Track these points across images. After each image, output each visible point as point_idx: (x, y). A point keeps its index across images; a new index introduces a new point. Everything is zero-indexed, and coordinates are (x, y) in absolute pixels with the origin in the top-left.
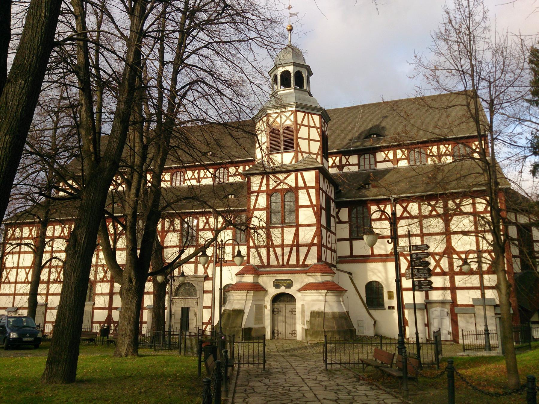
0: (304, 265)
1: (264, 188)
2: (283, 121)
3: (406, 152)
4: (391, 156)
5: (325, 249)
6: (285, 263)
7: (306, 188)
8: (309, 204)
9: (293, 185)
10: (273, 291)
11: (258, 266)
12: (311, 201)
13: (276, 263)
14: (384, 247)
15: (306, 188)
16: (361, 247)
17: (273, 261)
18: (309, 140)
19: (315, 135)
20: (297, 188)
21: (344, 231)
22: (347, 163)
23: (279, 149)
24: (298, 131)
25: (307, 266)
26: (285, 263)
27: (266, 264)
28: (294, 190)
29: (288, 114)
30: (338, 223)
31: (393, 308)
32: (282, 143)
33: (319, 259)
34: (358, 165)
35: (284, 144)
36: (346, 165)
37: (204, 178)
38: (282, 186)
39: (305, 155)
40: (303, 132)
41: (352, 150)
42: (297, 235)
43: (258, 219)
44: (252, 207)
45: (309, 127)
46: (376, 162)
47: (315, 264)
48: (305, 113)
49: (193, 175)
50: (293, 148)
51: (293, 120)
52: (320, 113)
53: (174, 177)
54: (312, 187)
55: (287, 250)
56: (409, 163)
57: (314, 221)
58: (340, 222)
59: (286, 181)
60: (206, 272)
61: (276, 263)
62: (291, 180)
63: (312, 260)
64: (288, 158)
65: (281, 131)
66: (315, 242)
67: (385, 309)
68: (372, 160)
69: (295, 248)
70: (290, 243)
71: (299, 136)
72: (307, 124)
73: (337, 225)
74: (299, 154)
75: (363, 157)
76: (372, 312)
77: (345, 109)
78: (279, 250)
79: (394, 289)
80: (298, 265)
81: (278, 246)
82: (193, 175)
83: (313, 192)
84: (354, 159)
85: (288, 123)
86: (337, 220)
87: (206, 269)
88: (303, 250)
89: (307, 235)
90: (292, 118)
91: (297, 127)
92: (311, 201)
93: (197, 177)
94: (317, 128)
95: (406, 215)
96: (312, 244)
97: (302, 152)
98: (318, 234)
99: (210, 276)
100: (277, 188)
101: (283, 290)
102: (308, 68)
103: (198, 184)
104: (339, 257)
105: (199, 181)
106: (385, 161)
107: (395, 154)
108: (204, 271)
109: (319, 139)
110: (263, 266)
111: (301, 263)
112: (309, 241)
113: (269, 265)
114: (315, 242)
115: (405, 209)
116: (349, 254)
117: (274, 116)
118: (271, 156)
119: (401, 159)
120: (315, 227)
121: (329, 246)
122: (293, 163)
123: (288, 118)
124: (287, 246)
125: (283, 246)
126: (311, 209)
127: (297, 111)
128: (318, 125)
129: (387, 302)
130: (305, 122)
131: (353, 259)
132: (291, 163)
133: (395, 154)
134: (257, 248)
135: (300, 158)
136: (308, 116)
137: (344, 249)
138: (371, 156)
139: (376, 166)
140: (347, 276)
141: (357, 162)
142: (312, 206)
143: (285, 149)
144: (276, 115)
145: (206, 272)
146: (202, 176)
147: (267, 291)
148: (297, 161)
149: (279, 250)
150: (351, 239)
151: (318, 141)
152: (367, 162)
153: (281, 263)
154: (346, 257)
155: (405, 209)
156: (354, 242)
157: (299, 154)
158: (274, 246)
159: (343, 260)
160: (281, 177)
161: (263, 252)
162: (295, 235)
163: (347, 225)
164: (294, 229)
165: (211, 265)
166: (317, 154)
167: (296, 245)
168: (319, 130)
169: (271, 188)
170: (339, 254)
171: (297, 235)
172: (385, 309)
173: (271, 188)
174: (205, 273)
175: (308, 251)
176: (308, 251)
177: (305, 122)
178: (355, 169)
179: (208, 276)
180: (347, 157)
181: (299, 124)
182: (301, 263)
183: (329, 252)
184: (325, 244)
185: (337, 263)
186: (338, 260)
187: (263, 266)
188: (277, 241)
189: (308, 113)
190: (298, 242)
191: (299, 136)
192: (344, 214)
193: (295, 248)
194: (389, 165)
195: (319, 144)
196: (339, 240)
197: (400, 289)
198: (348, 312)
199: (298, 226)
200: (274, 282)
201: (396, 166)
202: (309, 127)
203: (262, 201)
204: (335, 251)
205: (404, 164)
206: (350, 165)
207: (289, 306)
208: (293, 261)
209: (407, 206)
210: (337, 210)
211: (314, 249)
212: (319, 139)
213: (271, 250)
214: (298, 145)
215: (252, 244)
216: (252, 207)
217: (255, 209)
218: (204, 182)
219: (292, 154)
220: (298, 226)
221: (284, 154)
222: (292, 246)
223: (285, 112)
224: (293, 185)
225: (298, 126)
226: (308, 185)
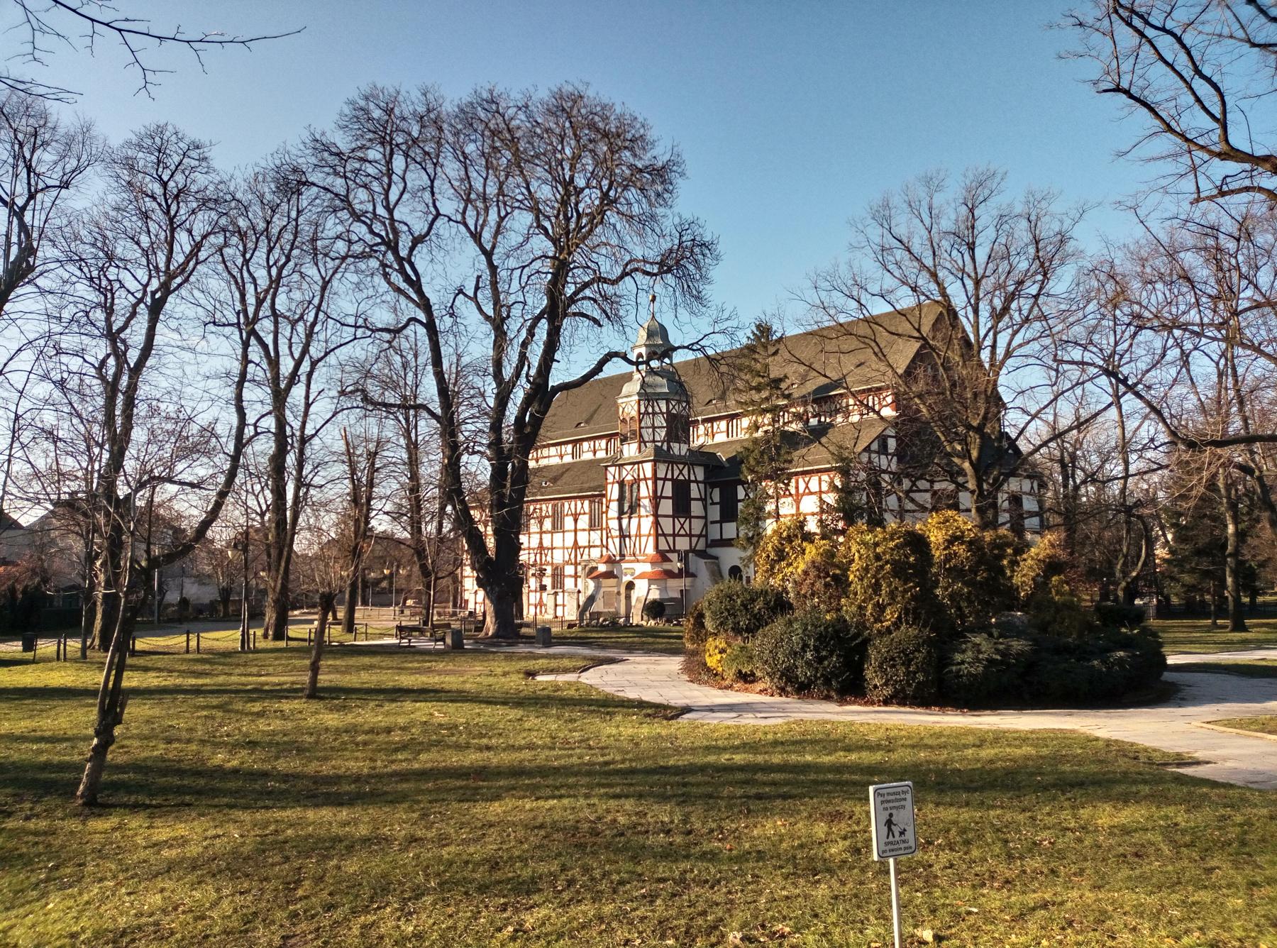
7: (645, 479)
16: (730, 530)
18: (654, 428)
19: (660, 421)
21: (715, 513)
24: (640, 421)
58: (713, 503)
88: (644, 540)
97: (645, 443)
128: (664, 410)
137: (714, 533)
150: (721, 522)
166: (663, 442)
196: (713, 522)
199: (640, 517)
203: (614, 492)
220: (640, 517)
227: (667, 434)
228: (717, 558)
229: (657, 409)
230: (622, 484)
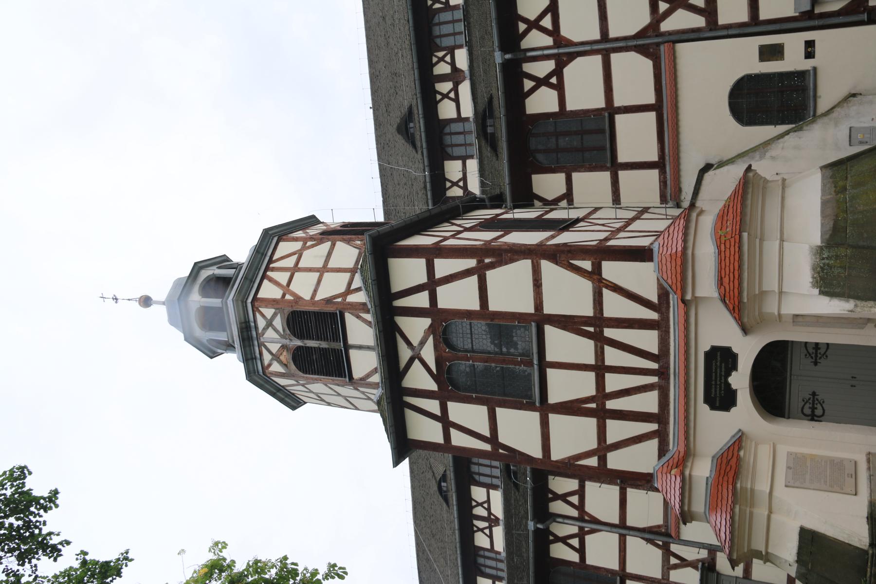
0: (661, 306)
1: (433, 406)
2: (276, 336)
3: (441, 54)
4: (445, 87)
5: (622, 235)
6: (654, 366)
7: (432, 285)
8: (474, 279)
9: (426, 322)
10: (745, 413)
11: (662, 451)
12: (467, 273)
13: (654, 395)
14: (634, 77)
15: (432, 285)
16: (636, 137)
17: (648, 402)
18: (324, 270)
20: (433, 311)
21: (591, 185)
22: (461, 184)
23: (337, 353)
24: (298, 299)
25: (663, 295)
26: (654, 366)
27: (654, 427)
28: (443, 322)
29: (261, 323)
30: (571, 202)
31: (810, 45)
32: (324, 345)
33: (641, 254)
34: (464, 159)
35: (325, 339)
36: (465, 188)
37: (489, 509)
38: (428, 353)
39: (357, 282)
40: (303, 286)
41: (431, 171)
42: (568, 323)
43: (519, 429)
44: (487, 447)
45: (296, 269)
46: (460, 119)
47: (660, 270)
48: (264, 276)
49: (482, 530)
50: (333, 315)
51: (272, 311)
52: (276, 239)
53: (488, 571)
55: (613, 357)
56: (460, 47)
57: (525, 266)
58: (568, 196)
59: (415, 342)
60: (693, 565)
61: (654, 395)
62: (415, 328)
63: (641, 278)
64: (360, 332)
65: (298, 343)
66: (587, 265)
67: (815, 69)
68: (456, 127)
69: (610, 333)
70: (590, 344)
71: (307, 296)
72: (287, 275)
73: (576, 205)
74: (351, 298)
75: (449, 150)
76: (823, 105)
77: (383, 197)
78: (613, 382)
79: (754, 43)
80: (660, 326)
81: (600, 383)
82: (482, 530)
83: (444, 267)
84: (453, 169)
85: (278, 323)
86: (564, 203)
87: (684, 563)
88: (615, 306)
89: (567, 292)
90: (269, 312)
91: (289, 301)
92: (467, 273)
93: (486, 524)
94: (304, 248)
95: (547, 22)
96: (595, 276)
97: (349, 291)
98: (563, 256)
99: (704, 554)
100: (433, 368)
101: (740, 380)
102: (198, 267)
103: (501, 523)
104: (663, 199)
105: (496, 521)
106: (457, 100)
107: (443, 78)
108: (689, 570)
109: (329, 243)
110: (661, 435)
111: (653, 315)
112: (586, 286)
113: (660, 418)
114: (587, 265)
115: (535, 25)
116: (655, 173)
117: (267, 357)
119: (453, 64)
120: (546, 266)
121: (618, 225)
122: (369, 317)
123: (269, 324)
124: (600, 354)
125: (600, 369)
126: (490, 274)
127: (255, 298)
128: (298, 245)
129: (793, 60)
130: (282, 277)
131: (666, 163)
132: (369, 323)
133: (443, 78)
134: (603, 449)
135: (360, 297)
136: (273, 269)
137: (641, 187)
138: (447, 130)
139: (467, 119)
140: (709, 176)
141: (459, 163)
142: (480, 271)
143: (336, 339)
144: (264, 351)
145: (693, 565)
146: (484, 513)
147: (740, 430)
149: (613, 382)
150: (615, 167)
151: (333, 245)
152: (459, 139)
153: (654, 379)
154: (663, 183)
155: (535, 25)
156: (622, 158)
157: (351, 298)
158: (602, 395)
159: (669, 193)
160: (405, 353)
161: (616, 430)
162: (564, 328)
163: (575, 176)
164: (549, 329)
165: (674, 548)
167: (593, 326)
168: (309, 243)
169: (433, 386)
170: (654, 198)
171: (568, 323)
172: (815, 69)
173: (433, 386)
174: (696, 568)
175: (616, 289)
176: (616, 289)
177: (282, 277)
178: (473, 165)
179: (703, 561)
180: (448, 184)
181: (284, 296)
182: (653, 315)
183: (637, 225)
184: (603, 236)
185: (678, 206)
186: (670, 204)
187: (661, 435)
188: (583, 386)
189: (267, 269)
190: (586, 321)
191: (307, 296)
192: (548, 184)
193: (609, 333)
194: (465, 89)
195: (340, 246)
197: (755, 25)
198: (823, 168)
200: (713, 407)
201: (467, 73)
202: (296, 269)
203: (469, 415)
204: (646, 210)
205: (462, 58)
206: (464, 178)
207: (799, 365)
208: (648, 340)
209: (525, 20)
210: (537, 203)
211: (612, 270)
212: (329, 243)
213: (611, 405)
214: (329, 301)
215: (593, 462)
216: (487, 447)
217: (493, 439)
218: (498, 509)
219: (349, 318)
220: (540, 319)
221: (351, 341)
222: (601, 341)
223: (256, 328)
224: (426, 322)
225: (288, 297)
226: (423, 279)
227: (348, 242)
228: (708, 167)
229: (290, 262)
230: (450, 386)
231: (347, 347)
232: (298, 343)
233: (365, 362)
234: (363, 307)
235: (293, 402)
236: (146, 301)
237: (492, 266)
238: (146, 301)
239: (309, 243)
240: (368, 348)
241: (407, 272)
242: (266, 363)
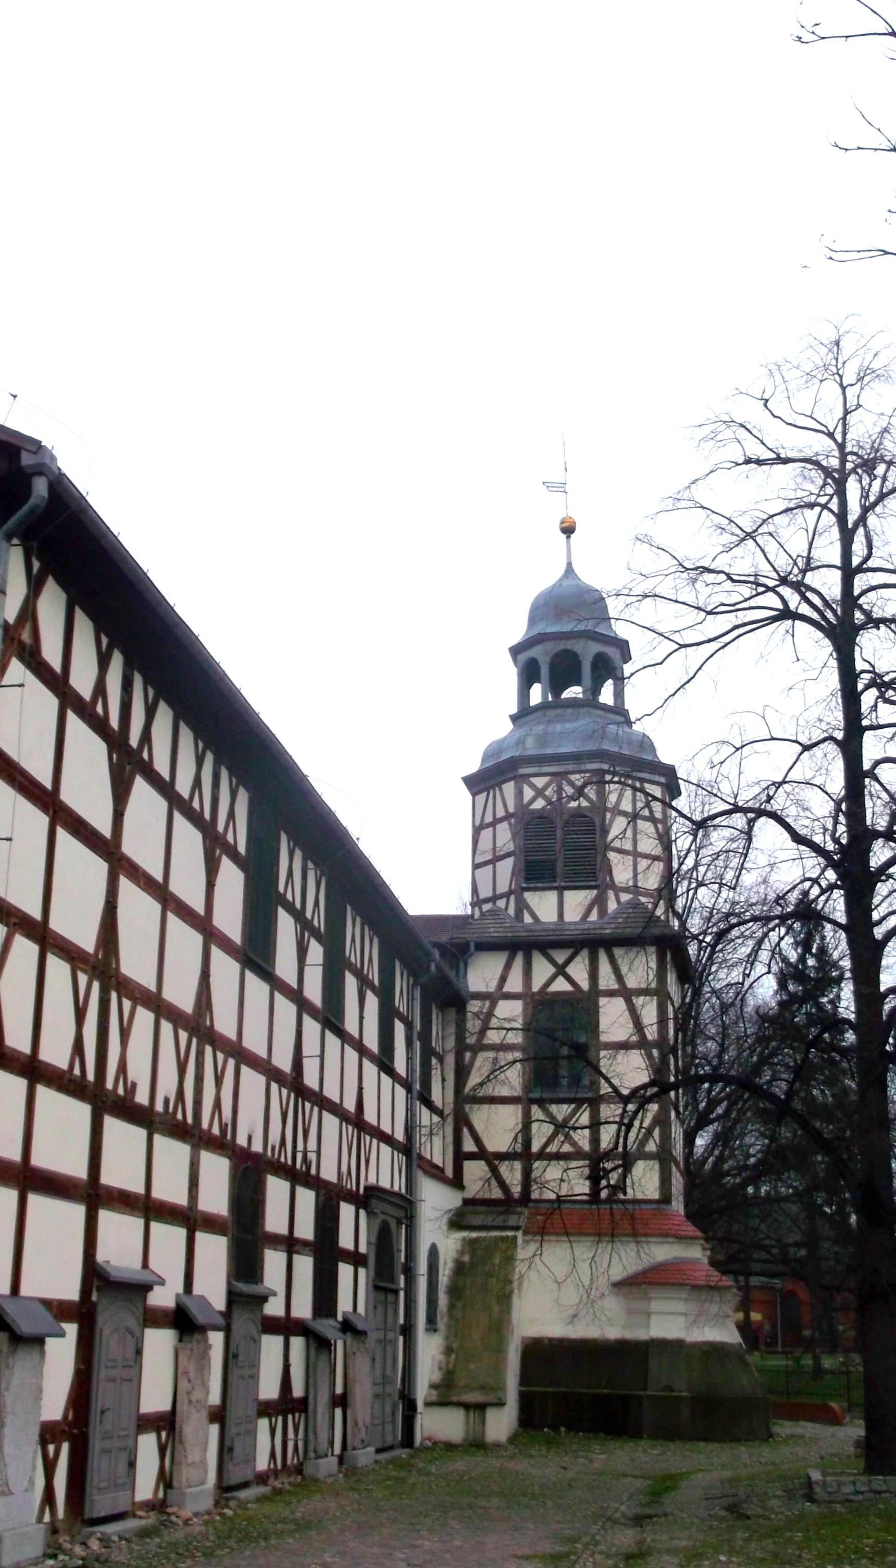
18: (636, 854)
39: (625, 897)
50: (593, 875)
54: (645, 992)
65: (559, 826)
74: (611, 894)
97: (618, 890)
117: (540, 782)
118: (527, 895)
122: (594, 916)
130: (626, 806)
135: (612, 906)
142: (643, 1044)
144: (546, 779)
148: (603, 912)
177: (626, 806)
217: (480, 1047)
225: (608, 815)
231: (561, 890)
232: (559, 826)
233: (544, 906)
234: (603, 912)
235: (477, 783)
236: (568, 530)
237: (650, 1056)
238: (568, 530)
239: (660, 826)
240: (561, 915)
241: (640, 969)
242: (534, 780)
